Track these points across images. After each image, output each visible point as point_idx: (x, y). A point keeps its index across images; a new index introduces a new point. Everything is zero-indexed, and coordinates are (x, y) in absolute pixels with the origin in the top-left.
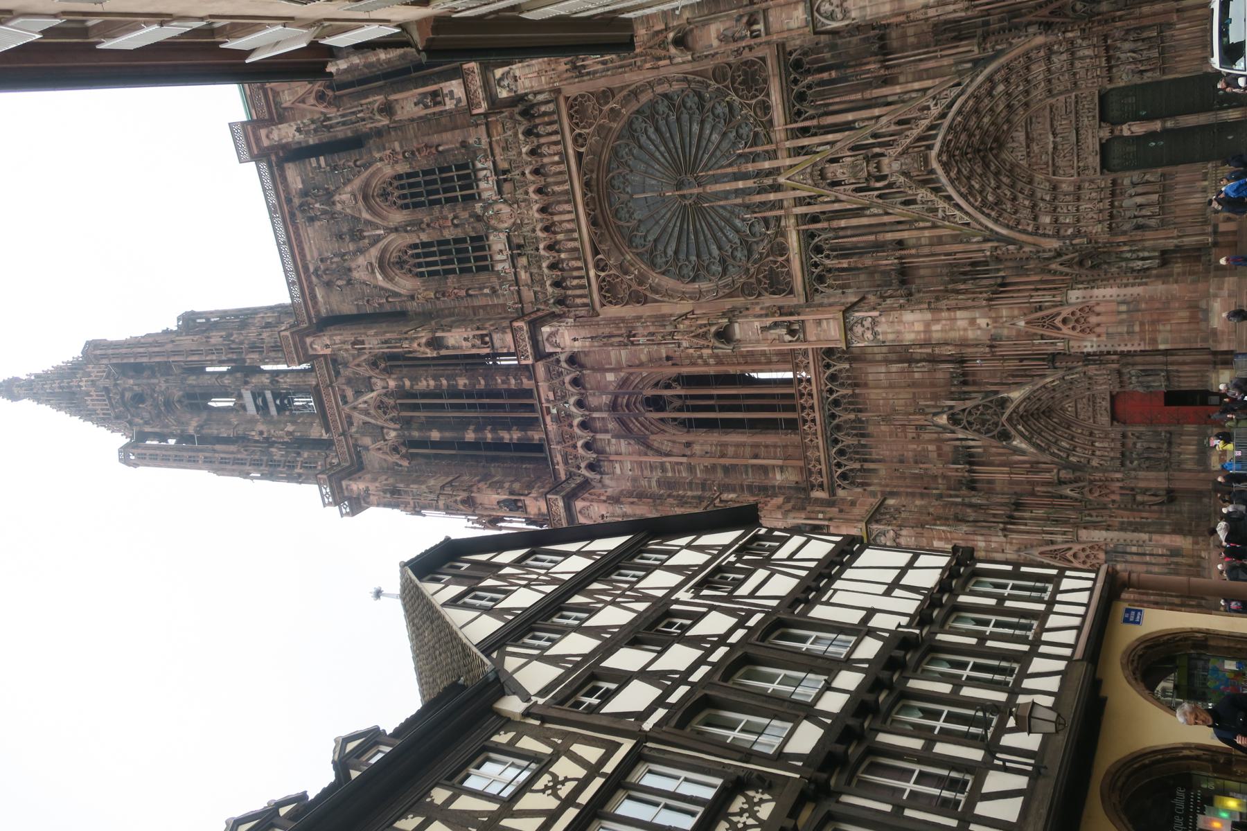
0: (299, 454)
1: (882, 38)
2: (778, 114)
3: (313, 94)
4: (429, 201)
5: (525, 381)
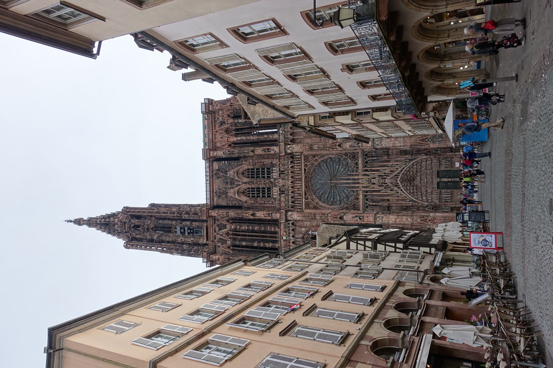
0: (193, 247)
1: (388, 152)
2: (360, 166)
5: (277, 229)
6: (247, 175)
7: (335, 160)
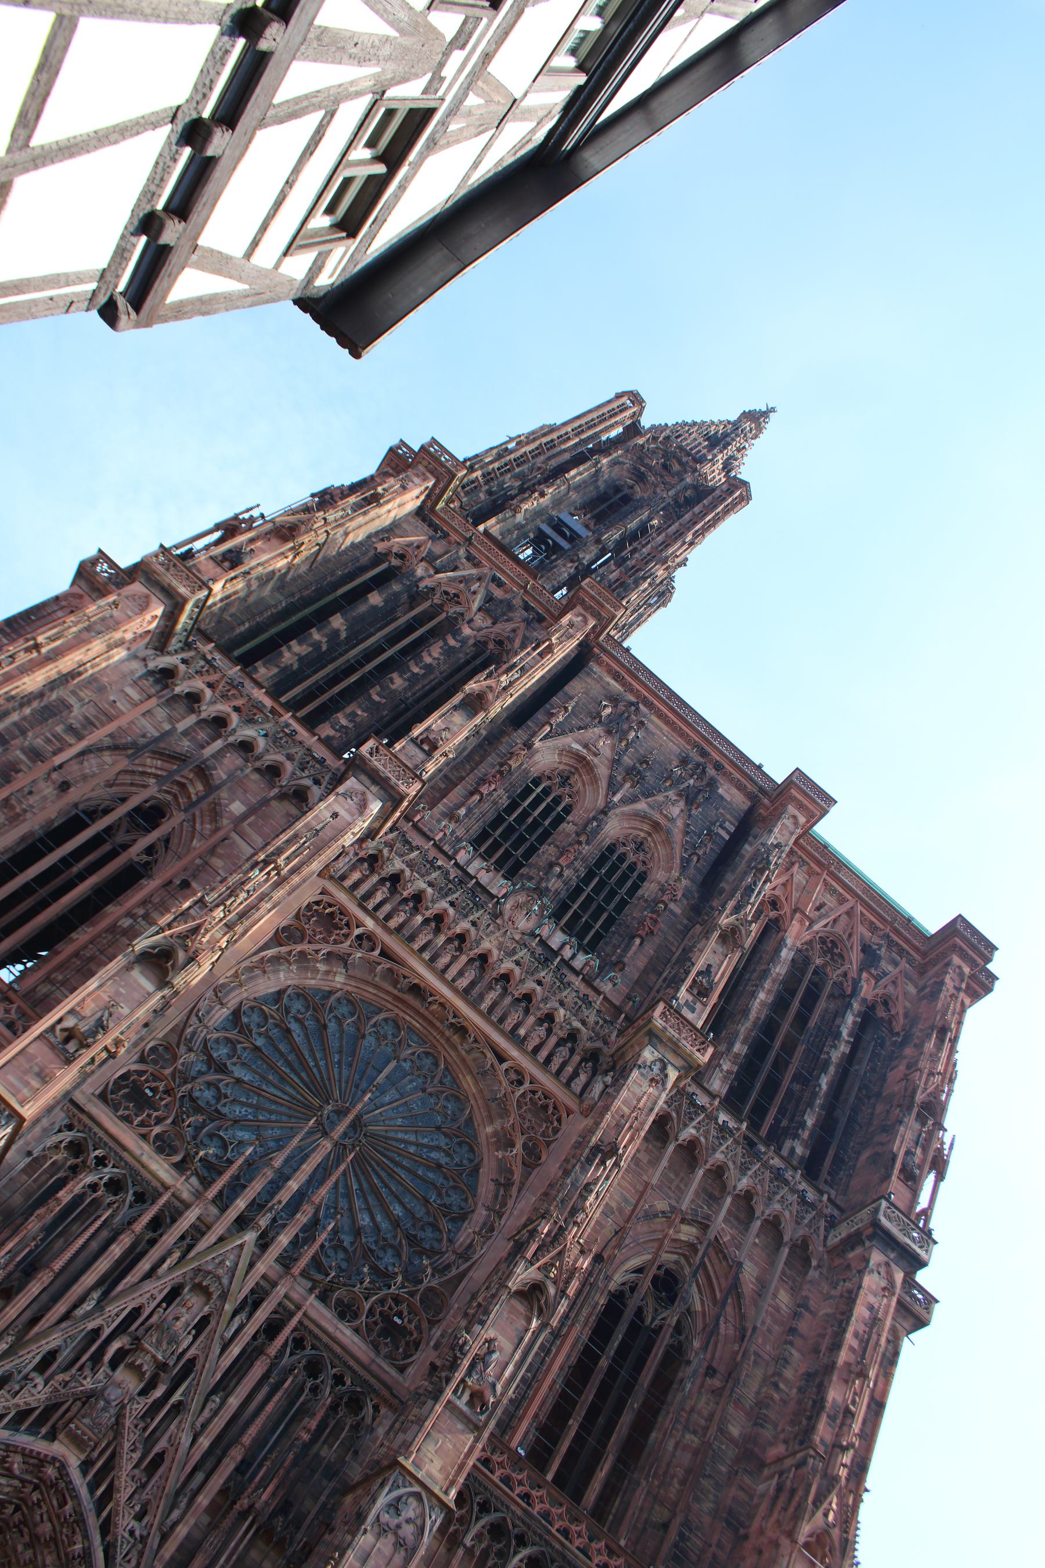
0: (490, 493)
1: (280, 1545)
3: (783, 899)
4: (595, 875)
5: (331, 732)
6: (624, 854)
7: (436, 1228)
